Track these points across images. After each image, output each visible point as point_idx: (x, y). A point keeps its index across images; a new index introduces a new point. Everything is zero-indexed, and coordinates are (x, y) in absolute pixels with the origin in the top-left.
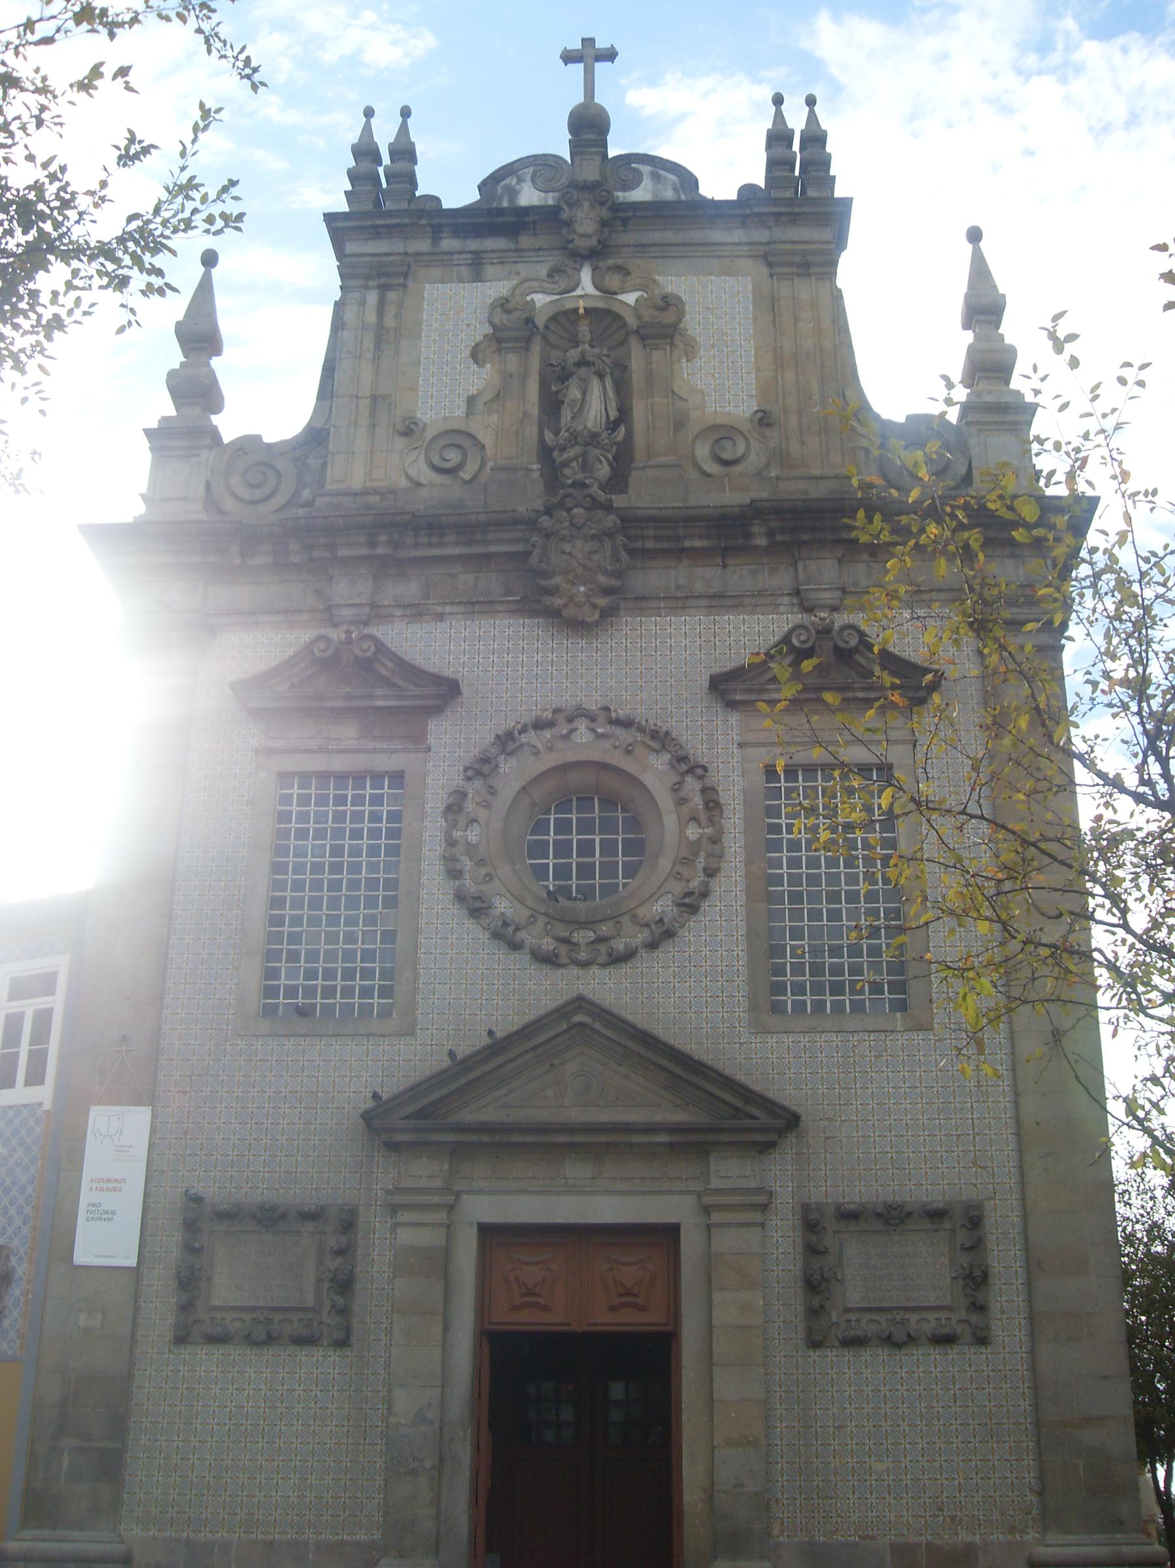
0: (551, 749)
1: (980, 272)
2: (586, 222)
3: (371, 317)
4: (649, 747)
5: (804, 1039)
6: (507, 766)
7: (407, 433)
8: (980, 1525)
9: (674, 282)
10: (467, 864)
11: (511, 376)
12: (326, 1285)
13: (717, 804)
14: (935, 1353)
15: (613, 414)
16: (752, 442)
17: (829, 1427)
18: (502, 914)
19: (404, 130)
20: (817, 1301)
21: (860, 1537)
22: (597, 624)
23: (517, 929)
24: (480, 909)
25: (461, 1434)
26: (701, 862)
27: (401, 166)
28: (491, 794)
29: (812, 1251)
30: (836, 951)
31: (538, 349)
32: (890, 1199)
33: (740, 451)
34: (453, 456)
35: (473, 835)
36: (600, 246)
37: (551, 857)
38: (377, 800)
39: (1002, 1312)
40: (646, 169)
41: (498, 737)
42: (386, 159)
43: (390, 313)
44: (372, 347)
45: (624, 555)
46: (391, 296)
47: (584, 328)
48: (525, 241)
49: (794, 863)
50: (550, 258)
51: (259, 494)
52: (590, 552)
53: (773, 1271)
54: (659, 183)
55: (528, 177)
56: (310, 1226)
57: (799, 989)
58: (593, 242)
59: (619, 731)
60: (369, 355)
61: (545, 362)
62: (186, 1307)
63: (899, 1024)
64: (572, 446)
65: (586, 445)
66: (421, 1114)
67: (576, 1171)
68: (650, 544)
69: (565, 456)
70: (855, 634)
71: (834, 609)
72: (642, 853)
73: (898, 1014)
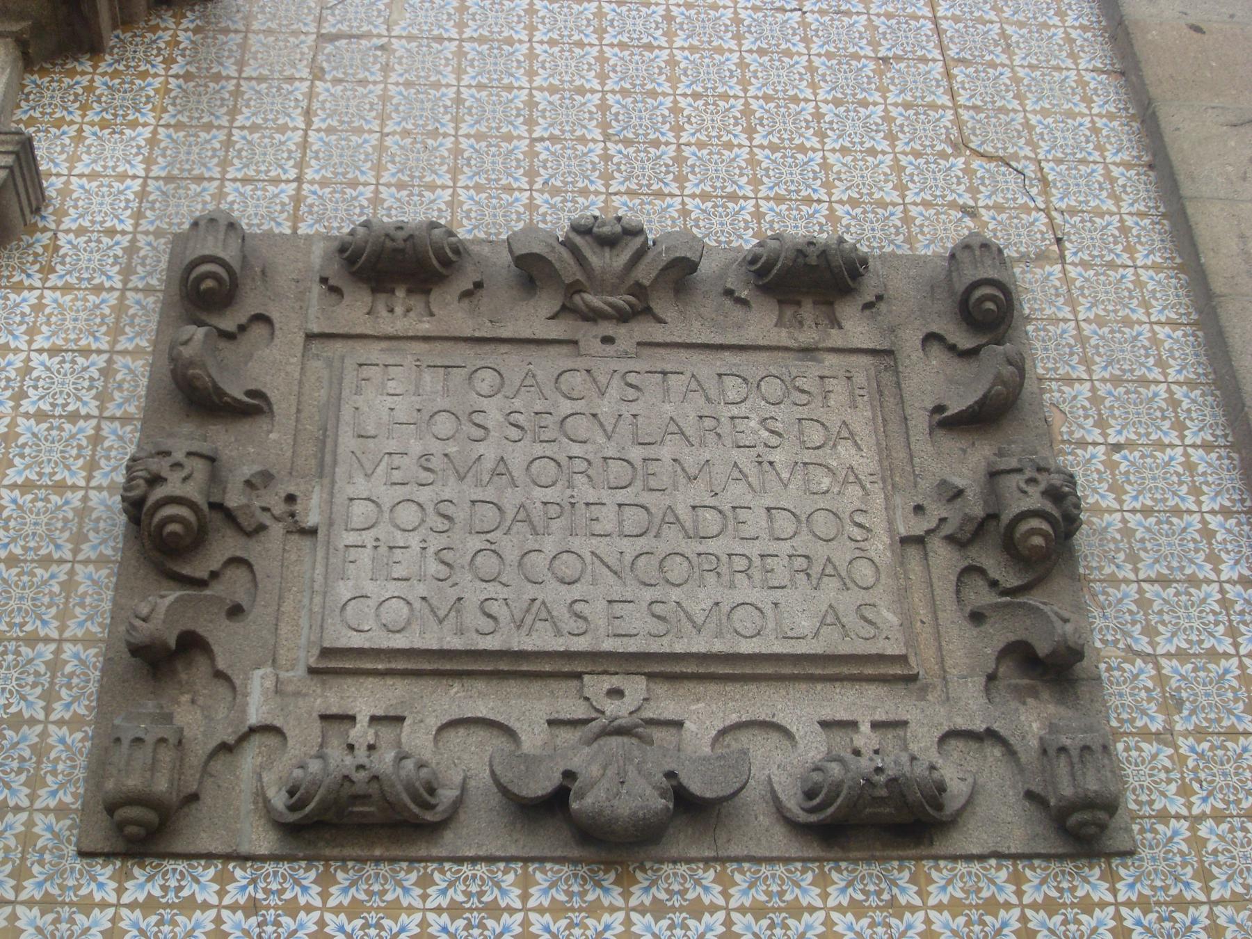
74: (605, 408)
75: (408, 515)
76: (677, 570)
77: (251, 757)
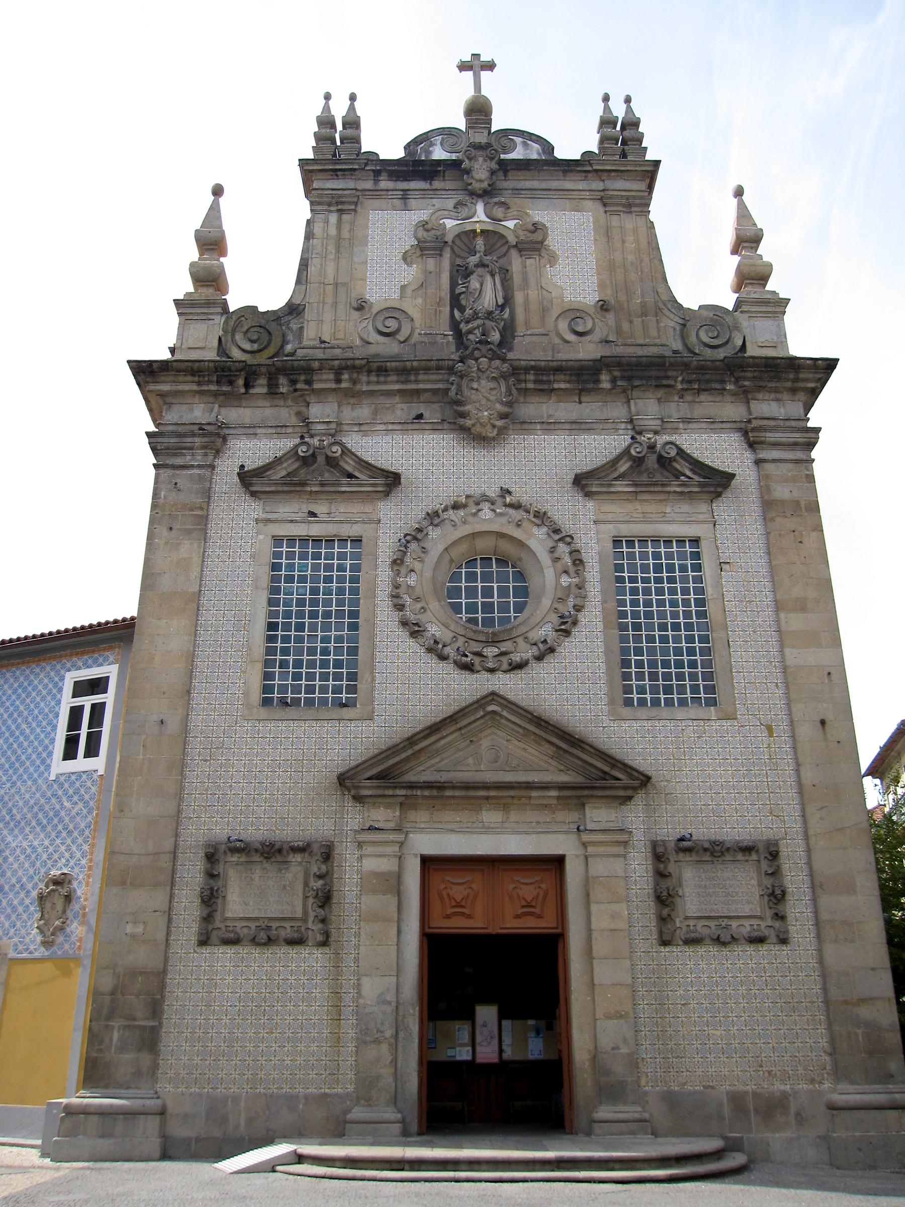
0: (465, 523)
1: (743, 214)
2: (481, 171)
3: (333, 231)
4: (533, 522)
5: (647, 725)
6: (434, 533)
7: (360, 309)
8: (789, 1078)
9: (539, 214)
10: (407, 600)
11: (430, 273)
12: (311, 900)
13: (581, 561)
14: (750, 949)
15: (500, 301)
16: (596, 320)
17: (677, 1004)
18: (433, 635)
19: (352, 108)
20: (665, 912)
21: (703, 1086)
22: (494, 439)
23: (444, 646)
24: (418, 631)
25: (411, 1011)
26: (571, 602)
27: (350, 132)
28: (424, 552)
29: (661, 875)
30: (666, 664)
31: (449, 256)
32: (713, 838)
33: (589, 325)
34: (392, 324)
35: (412, 580)
36: (490, 188)
37: (463, 598)
38: (342, 556)
39: (797, 921)
40: (518, 140)
41: (428, 514)
42: (339, 127)
43: (346, 228)
44: (333, 252)
45: (514, 392)
46: (346, 217)
47: (480, 243)
48: (437, 184)
49: (635, 603)
50: (456, 196)
51: (256, 346)
52: (491, 389)
53: (632, 889)
54: (528, 149)
55: (438, 142)
56: (298, 857)
57: (642, 690)
58: (485, 185)
59: (511, 511)
60: (332, 256)
61: (452, 265)
62: (207, 919)
63: (713, 714)
64: (475, 320)
65: (486, 318)
66: (379, 776)
67: (491, 817)
68: (531, 386)
69: (470, 326)
70: (674, 447)
71: (656, 433)
72: (526, 595)
73: (712, 708)
74: (719, 875)
75: (694, 895)
76: (730, 902)
77: (678, 931)
